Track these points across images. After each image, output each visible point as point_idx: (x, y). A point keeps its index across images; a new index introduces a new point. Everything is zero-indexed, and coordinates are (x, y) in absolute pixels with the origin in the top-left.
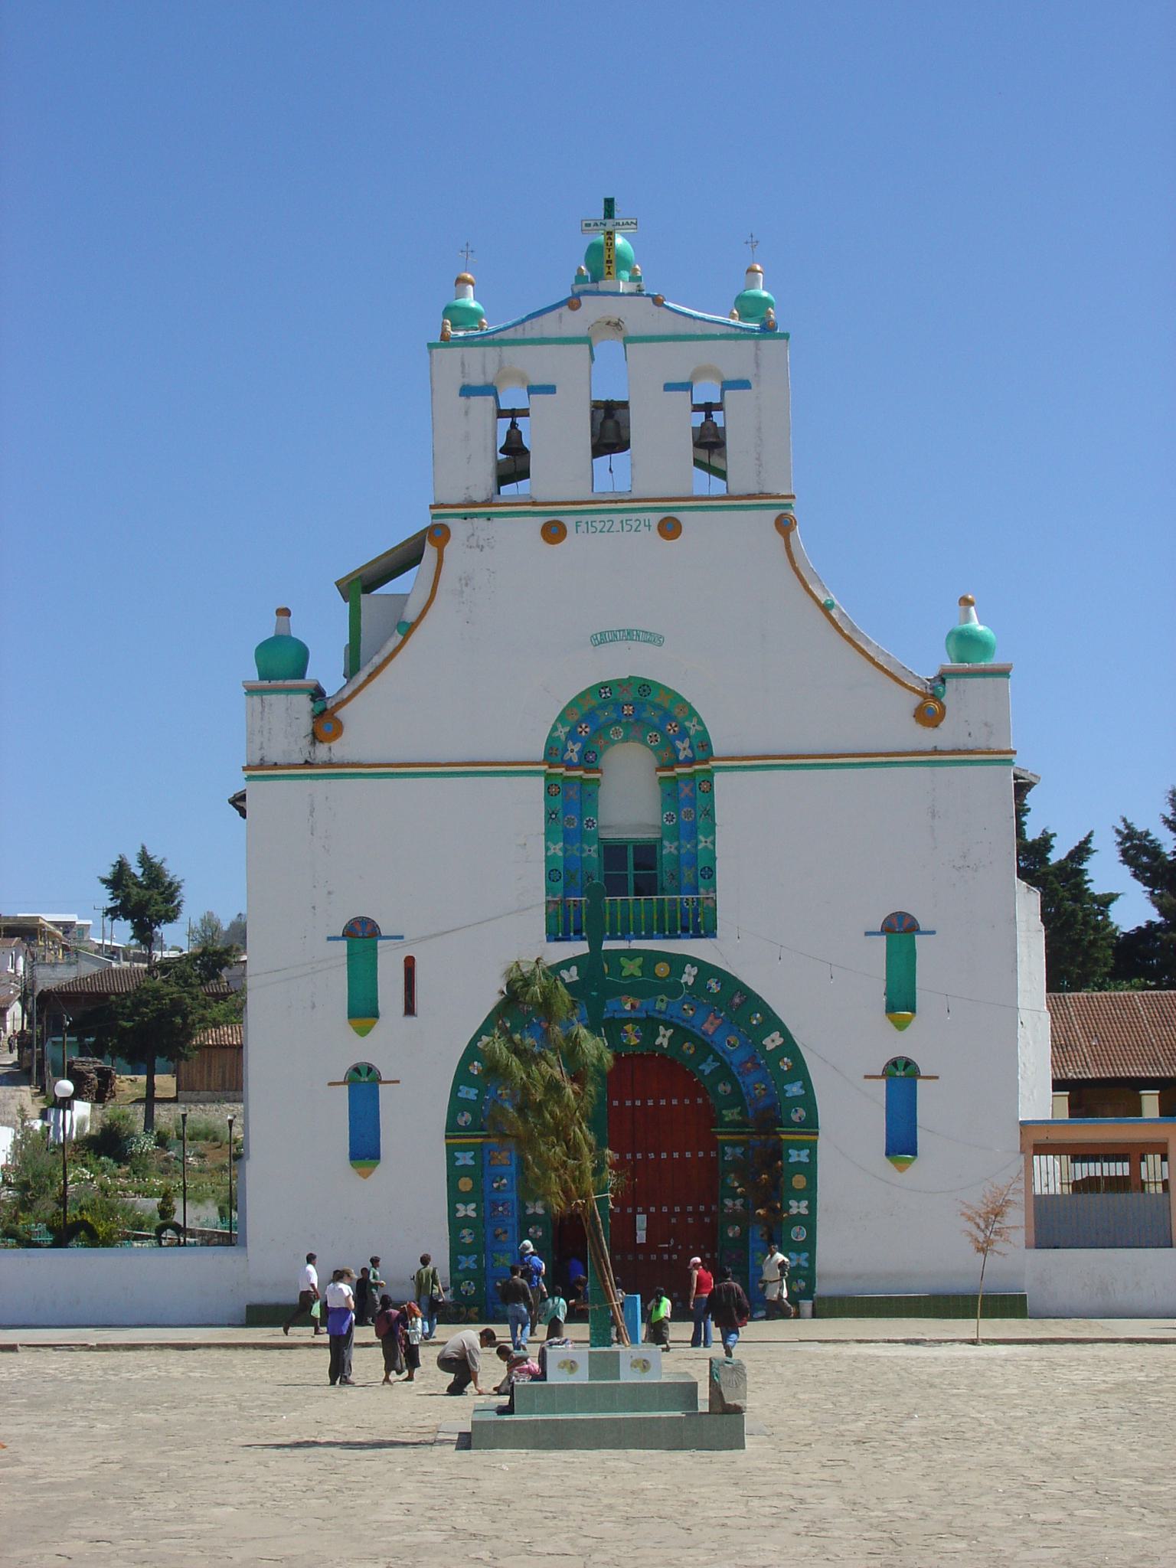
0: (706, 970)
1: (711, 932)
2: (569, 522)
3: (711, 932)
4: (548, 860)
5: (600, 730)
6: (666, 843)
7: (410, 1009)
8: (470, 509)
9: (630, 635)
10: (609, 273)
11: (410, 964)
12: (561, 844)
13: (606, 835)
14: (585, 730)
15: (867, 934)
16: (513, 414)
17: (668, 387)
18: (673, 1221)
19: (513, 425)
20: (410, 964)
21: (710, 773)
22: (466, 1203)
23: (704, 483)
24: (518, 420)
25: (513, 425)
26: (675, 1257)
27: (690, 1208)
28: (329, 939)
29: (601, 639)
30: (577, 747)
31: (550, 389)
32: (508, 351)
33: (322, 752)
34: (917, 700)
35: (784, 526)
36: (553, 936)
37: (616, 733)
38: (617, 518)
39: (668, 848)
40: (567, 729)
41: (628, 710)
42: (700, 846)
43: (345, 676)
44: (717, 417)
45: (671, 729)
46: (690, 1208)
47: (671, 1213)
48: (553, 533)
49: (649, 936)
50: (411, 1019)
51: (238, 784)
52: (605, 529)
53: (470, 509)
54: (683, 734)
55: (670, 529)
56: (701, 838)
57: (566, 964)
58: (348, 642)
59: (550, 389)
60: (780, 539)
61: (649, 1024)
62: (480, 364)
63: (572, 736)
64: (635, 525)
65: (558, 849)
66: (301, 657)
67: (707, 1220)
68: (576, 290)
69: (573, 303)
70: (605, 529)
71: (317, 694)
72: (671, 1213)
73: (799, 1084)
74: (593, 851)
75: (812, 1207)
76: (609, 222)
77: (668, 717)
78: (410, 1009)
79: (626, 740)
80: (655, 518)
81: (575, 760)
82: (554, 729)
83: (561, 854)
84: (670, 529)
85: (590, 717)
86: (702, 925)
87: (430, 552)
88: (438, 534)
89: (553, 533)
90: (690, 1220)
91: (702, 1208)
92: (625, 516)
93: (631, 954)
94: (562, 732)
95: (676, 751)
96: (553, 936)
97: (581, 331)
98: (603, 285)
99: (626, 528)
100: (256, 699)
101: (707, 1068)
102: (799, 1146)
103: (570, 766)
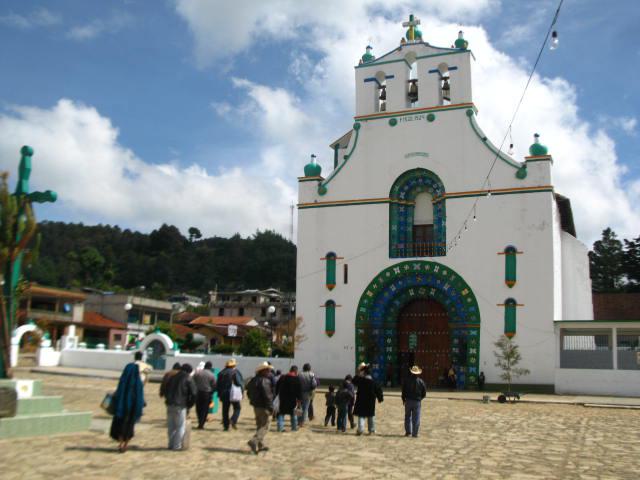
0: (443, 267)
1: (442, 253)
2: (398, 118)
3: (442, 253)
5: (412, 188)
7: (346, 281)
8: (367, 118)
9: (418, 154)
11: (346, 267)
13: (416, 223)
14: (406, 188)
17: (431, 72)
20: (346, 267)
21: (444, 200)
23: (446, 103)
29: (408, 156)
31: (392, 77)
34: (516, 170)
35: (470, 114)
36: (391, 256)
37: (419, 189)
38: (413, 116)
41: (420, 180)
44: (449, 81)
48: (393, 123)
49: (423, 256)
50: (345, 285)
53: (367, 118)
55: (431, 119)
57: (395, 266)
59: (392, 77)
60: (467, 118)
61: (428, 287)
62: (371, 72)
63: (401, 189)
66: (318, 170)
69: (399, 49)
71: (321, 179)
74: (410, 229)
75: (478, 351)
77: (433, 182)
78: (346, 281)
79: (422, 192)
80: (426, 114)
82: (393, 187)
84: (431, 119)
85: (407, 183)
89: (393, 123)
93: (417, 262)
94: (397, 188)
96: (391, 256)
101: (447, 302)
102: (474, 329)
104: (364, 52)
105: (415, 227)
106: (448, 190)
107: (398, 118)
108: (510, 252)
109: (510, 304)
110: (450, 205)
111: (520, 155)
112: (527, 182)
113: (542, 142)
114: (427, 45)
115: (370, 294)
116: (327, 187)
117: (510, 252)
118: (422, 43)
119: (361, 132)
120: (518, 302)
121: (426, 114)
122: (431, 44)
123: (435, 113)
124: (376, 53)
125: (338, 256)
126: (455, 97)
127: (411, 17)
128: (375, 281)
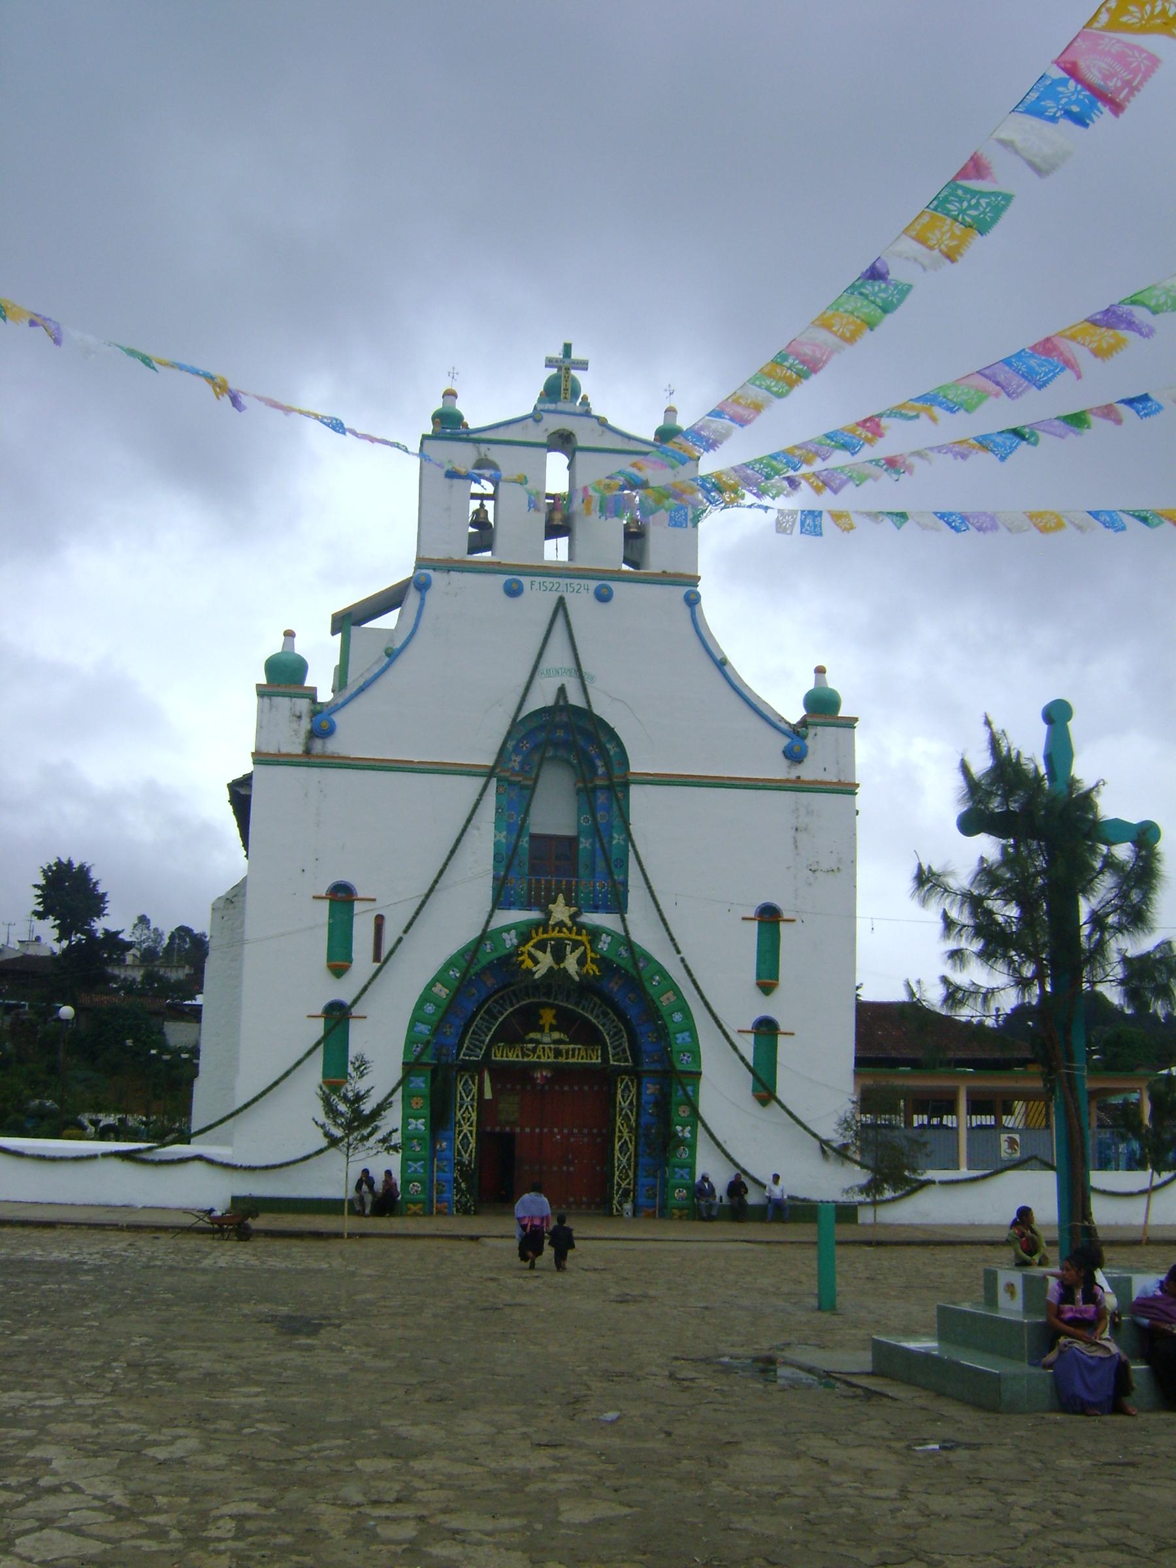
4: (497, 844)
6: (582, 839)
8: (449, 566)
10: (565, 398)
11: (380, 921)
12: (505, 833)
14: (527, 746)
15: (744, 919)
16: (482, 497)
18: (572, 1140)
19: (482, 505)
20: (380, 921)
21: (626, 785)
22: (417, 1118)
24: (485, 502)
25: (482, 505)
26: (572, 1169)
27: (585, 1131)
28: (314, 897)
30: (519, 759)
32: (483, 447)
33: (318, 746)
34: (785, 741)
35: (693, 601)
39: (585, 844)
40: (514, 743)
42: (615, 842)
43: (333, 691)
45: (592, 751)
46: (585, 1131)
47: (571, 1134)
51: (245, 766)
52: (554, 589)
53: (449, 566)
54: (603, 753)
56: (615, 835)
58: (338, 663)
60: (687, 611)
62: (463, 456)
63: (517, 750)
64: (577, 588)
65: (502, 836)
67: (599, 1140)
68: (540, 407)
69: (536, 417)
70: (554, 589)
72: (572, 1134)
73: (687, 1034)
74: (525, 842)
76: (567, 361)
81: (517, 768)
83: (504, 841)
84: (603, 596)
85: (530, 734)
86: (617, 903)
87: (413, 598)
88: (420, 584)
90: (586, 1140)
91: (595, 1131)
92: (568, 581)
95: (594, 768)
97: (544, 440)
98: (561, 406)
99: (570, 589)
100: (266, 700)
103: (514, 773)
104: (438, 405)
105: (533, 837)
106: (636, 766)
107: (525, 581)
108: (769, 917)
109: (766, 1029)
110: (638, 796)
111: (794, 713)
112: (808, 771)
113: (833, 682)
114: (602, 422)
115: (442, 992)
116: (337, 718)
117: (769, 917)
118: (587, 414)
119: (430, 595)
120: (783, 1027)
121: (593, 584)
122: (610, 422)
123: (613, 585)
124: (474, 420)
125: (361, 894)
126: (658, 559)
127: (567, 348)
128: (450, 964)
